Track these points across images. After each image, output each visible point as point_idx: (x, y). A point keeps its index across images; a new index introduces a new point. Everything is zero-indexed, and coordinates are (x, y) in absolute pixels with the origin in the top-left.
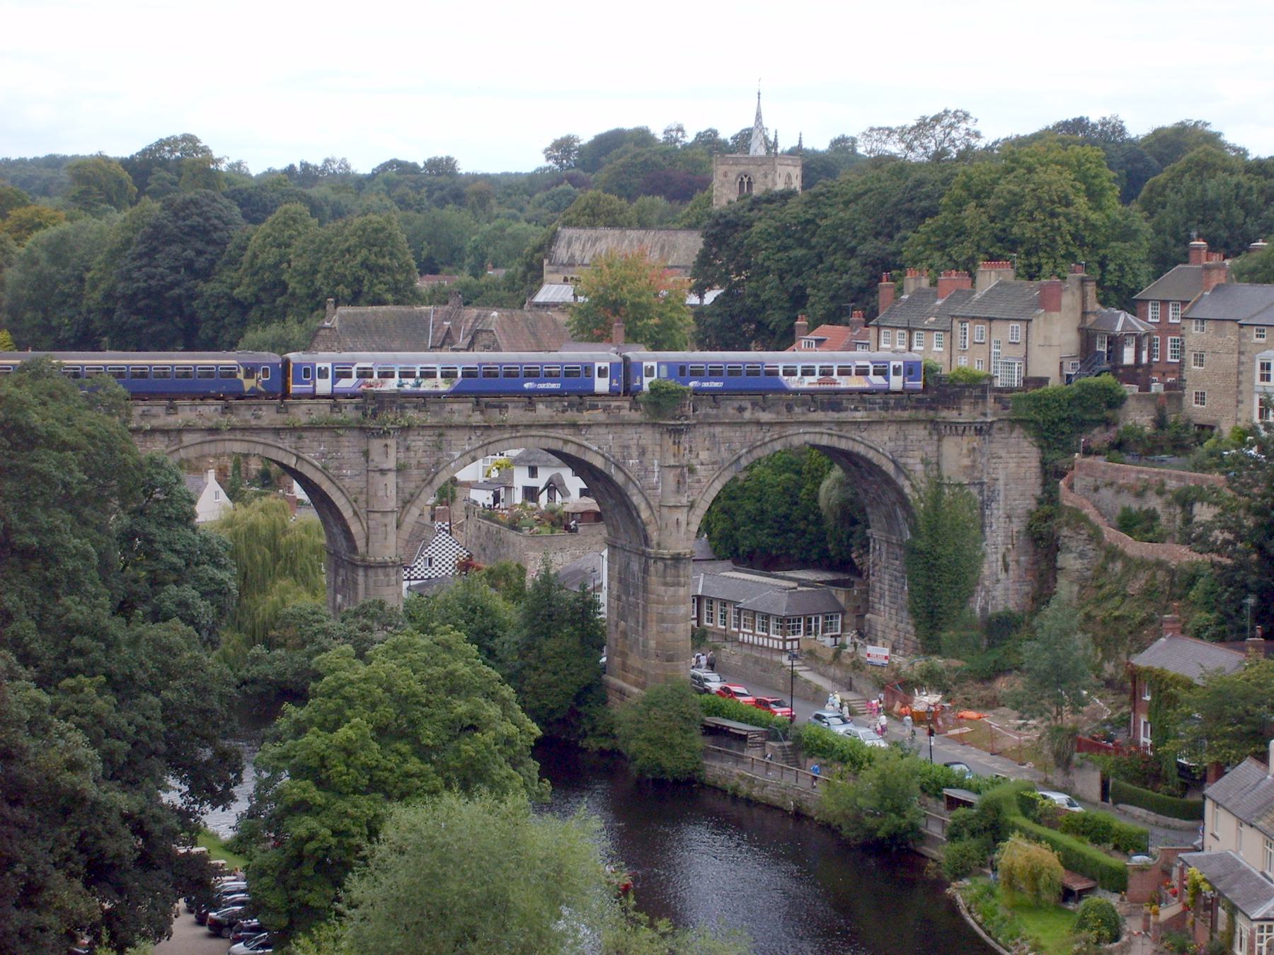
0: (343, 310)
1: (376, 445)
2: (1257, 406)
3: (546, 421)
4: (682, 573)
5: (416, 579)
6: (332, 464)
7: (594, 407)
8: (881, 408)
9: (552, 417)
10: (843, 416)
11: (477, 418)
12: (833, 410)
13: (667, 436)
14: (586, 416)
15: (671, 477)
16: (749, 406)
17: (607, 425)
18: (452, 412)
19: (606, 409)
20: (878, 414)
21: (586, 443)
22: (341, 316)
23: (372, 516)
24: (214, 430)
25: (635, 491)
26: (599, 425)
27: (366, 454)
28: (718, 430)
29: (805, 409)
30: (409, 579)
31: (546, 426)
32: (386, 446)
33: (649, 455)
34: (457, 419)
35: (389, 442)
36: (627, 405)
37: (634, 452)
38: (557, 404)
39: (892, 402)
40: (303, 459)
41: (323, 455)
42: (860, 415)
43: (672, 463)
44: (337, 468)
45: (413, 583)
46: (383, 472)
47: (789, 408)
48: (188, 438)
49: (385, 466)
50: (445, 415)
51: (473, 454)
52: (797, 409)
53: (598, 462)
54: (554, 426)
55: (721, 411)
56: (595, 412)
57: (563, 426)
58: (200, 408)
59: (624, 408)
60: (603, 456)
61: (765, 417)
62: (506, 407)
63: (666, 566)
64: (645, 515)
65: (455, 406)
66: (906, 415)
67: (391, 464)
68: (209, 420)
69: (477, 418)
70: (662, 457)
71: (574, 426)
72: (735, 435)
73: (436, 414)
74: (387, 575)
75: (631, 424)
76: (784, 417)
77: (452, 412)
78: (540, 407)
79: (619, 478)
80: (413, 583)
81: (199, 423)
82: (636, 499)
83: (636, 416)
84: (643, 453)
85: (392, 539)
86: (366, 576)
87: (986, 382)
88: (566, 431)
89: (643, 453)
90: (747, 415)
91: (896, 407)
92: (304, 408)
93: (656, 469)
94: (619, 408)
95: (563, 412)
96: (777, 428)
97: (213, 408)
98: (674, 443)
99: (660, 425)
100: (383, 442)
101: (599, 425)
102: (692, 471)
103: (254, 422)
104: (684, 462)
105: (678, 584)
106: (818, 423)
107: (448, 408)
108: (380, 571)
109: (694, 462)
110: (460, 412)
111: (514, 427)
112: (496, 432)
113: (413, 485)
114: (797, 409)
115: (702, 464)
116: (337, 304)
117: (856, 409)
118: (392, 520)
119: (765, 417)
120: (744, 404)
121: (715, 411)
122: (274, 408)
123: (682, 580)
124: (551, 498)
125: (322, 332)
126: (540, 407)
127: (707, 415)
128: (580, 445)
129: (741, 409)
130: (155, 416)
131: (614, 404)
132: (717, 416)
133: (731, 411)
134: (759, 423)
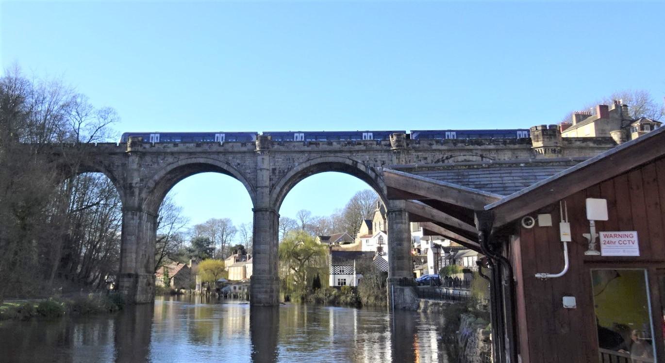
4: (403, 217)
8: (503, 144)
9: (340, 148)
10: (483, 147)
12: (477, 145)
16: (434, 143)
20: (501, 146)
24: (191, 153)
25: (381, 181)
29: (463, 145)
31: (336, 152)
32: (263, 159)
35: (264, 157)
37: (380, 165)
39: (508, 141)
42: (492, 147)
47: (455, 144)
49: (262, 167)
52: (460, 145)
54: (341, 152)
56: (361, 146)
59: (373, 144)
62: (319, 144)
63: (396, 215)
66: (517, 146)
71: (350, 152)
72: (429, 156)
75: (377, 151)
76: (453, 147)
79: (373, 175)
87: (555, 128)
90: (435, 147)
91: (510, 143)
94: (371, 144)
95: (345, 146)
96: (450, 154)
105: (402, 223)
106: (471, 150)
108: (260, 213)
117: (489, 144)
121: (418, 145)
123: (404, 221)
129: (431, 144)
132: (419, 147)
134: (440, 150)
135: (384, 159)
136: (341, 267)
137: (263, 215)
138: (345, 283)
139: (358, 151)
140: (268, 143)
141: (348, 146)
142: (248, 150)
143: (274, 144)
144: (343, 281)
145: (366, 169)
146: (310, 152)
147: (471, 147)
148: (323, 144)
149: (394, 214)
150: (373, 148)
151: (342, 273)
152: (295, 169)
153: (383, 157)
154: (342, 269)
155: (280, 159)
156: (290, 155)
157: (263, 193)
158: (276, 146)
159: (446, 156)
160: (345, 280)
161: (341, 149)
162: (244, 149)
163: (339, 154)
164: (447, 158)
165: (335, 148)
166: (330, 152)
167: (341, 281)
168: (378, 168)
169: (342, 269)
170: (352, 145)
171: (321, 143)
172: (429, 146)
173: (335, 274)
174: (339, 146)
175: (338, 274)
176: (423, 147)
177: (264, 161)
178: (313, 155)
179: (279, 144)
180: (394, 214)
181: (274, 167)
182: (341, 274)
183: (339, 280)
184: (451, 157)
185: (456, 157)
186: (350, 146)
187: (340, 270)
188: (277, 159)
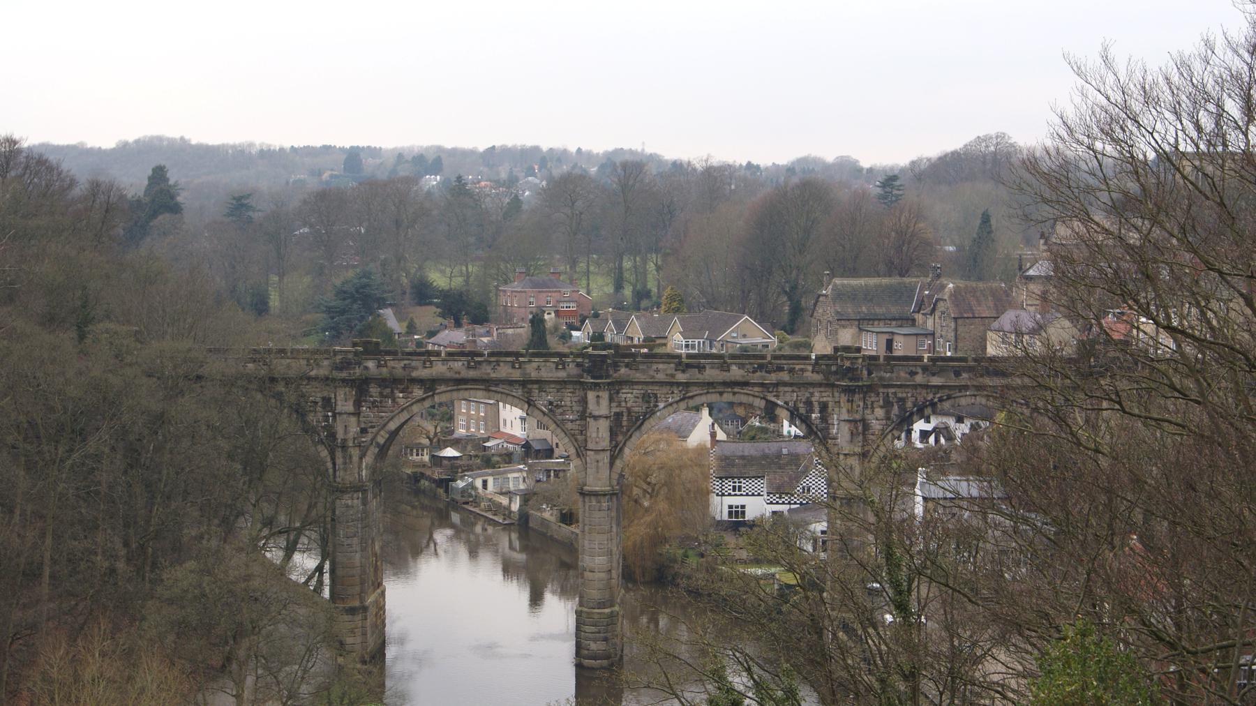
0: (838, 281)
1: (591, 395)
2: (720, 390)
3: (741, 379)
5: (795, 503)
7: (780, 369)
9: (743, 376)
11: (681, 377)
13: (843, 395)
14: (773, 378)
15: (846, 428)
16: (919, 370)
17: (791, 385)
18: (657, 371)
19: (791, 371)
21: (774, 399)
22: (835, 285)
23: (589, 453)
26: (785, 384)
27: (584, 401)
30: (789, 503)
34: (661, 377)
35: (600, 394)
36: (810, 368)
37: (817, 409)
38: (748, 366)
40: (535, 406)
41: (551, 403)
43: (847, 418)
44: (561, 414)
45: (793, 506)
46: (596, 418)
48: (442, 388)
49: (596, 413)
50: (652, 373)
51: (675, 406)
52: (965, 375)
54: (745, 384)
55: (894, 375)
57: (755, 385)
58: (450, 363)
60: (788, 409)
61: (936, 381)
62: (704, 367)
65: (661, 366)
67: (603, 409)
68: (459, 373)
69: (681, 377)
70: (839, 415)
73: (644, 372)
74: (599, 502)
77: (657, 371)
78: (734, 368)
80: (793, 506)
81: (449, 375)
83: (818, 378)
84: (824, 407)
85: (605, 473)
88: (756, 389)
89: (824, 407)
90: (919, 379)
92: (535, 365)
94: (802, 370)
95: (754, 372)
96: (947, 392)
97: (460, 363)
98: (848, 401)
99: (838, 386)
100: (597, 394)
101: (785, 384)
102: (866, 427)
103: (493, 375)
104: (858, 417)
107: (654, 367)
108: (593, 499)
109: (869, 417)
110: (666, 370)
111: (710, 384)
112: (695, 388)
114: (965, 375)
115: (877, 419)
116: (833, 275)
118: (605, 458)
119: (936, 381)
120: (914, 369)
121: (888, 375)
122: (510, 364)
124: (937, 441)
125: (821, 299)
126: (734, 368)
127: (881, 379)
129: (913, 374)
130: (415, 368)
131: (797, 367)
132: (890, 379)
133: (902, 374)
135: (825, 399)
136: (736, 480)
137: (599, 502)
138: (743, 513)
139: (777, 385)
140: (607, 367)
141: (758, 374)
142: (569, 376)
143: (619, 366)
144: (740, 509)
146: (687, 385)
147: (988, 381)
148: (712, 368)
149: (838, 503)
150: (807, 377)
151: (739, 493)
152: (658, 414)
153: (824, 394)
154: (737, 484)
155: (629, 395)
156: (651, 389)
157: (598, 461)
158: (623, 370)
159: (938, 395)
160: (743, 507)
161: (746, 379)
162: (562, 374)
164: (941, 400)
166: (726, 384)
167: (734, 509)
168: (813, 415)
169: (737, 484)
170: (766, 372)
171: (707, 366)
172: (908, 376)
173: (723, 495)
174: (742, 372)
175: (730, 495)
176: (898, 378)
177: (601, 400)
179: (627, 366)
180: (838, 503)
181: (618, 410)
182: (736, 495)
183: (731, 507)
184: (949, 397)
185: (957, 400)
186: (764, 374)
187: (734, 490)
188: (625, 396)
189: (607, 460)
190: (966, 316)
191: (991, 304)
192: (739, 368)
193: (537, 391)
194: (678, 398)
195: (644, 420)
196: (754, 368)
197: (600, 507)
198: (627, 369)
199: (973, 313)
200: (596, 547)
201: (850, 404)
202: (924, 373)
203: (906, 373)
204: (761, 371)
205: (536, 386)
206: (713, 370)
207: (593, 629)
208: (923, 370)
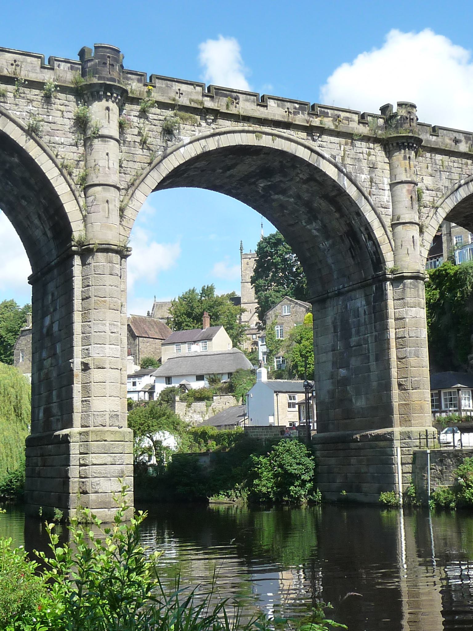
6: (45, 128)
9: (283, 117)
25: (369, 208)
28: (438, 157)
32: (108, 109)
33: (378, 172)
44: (48, 134)
53: (331, 172)
54: (287, 125)
64: (378, 233)
70: (392, 175)
79: (352, 191)
82: (370, 216)
84: (373, 168)
86: (84, 264)
89: (373, 168)
93: (387, 187)
94: (347, 119)
95: (295, 113)
98: (405, 158)
113: (137, 166)
128: (312, 151)
129: (457, 141)
133: (447, 141)
145: (338, 175)
148: (247, 100)
150: (353, 128)
163: (286, 133)
165: (274, 115)
168: (363, 177)
178: (226, 125)
189: (115, 206)
190: (144, 336)
191: (157, 330)
192: (278, 106)
193: (11, 95)
194: (208, 133)
195: (165, 157)
196: (295, 108)
197: (112, 269)
198: (141, 85)
199: (148, 335)
200: (107, 329)
201: (407, 162)
202: (467, 143)
203: (451, 139)
204: (303, 114)
205: (10, 88)
206: (248, 104)
207: (107, 458)
208: (465, 138)
